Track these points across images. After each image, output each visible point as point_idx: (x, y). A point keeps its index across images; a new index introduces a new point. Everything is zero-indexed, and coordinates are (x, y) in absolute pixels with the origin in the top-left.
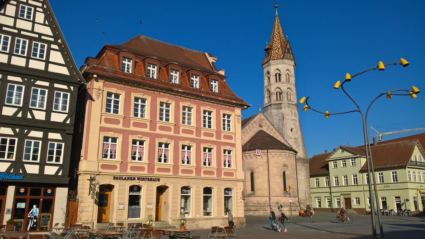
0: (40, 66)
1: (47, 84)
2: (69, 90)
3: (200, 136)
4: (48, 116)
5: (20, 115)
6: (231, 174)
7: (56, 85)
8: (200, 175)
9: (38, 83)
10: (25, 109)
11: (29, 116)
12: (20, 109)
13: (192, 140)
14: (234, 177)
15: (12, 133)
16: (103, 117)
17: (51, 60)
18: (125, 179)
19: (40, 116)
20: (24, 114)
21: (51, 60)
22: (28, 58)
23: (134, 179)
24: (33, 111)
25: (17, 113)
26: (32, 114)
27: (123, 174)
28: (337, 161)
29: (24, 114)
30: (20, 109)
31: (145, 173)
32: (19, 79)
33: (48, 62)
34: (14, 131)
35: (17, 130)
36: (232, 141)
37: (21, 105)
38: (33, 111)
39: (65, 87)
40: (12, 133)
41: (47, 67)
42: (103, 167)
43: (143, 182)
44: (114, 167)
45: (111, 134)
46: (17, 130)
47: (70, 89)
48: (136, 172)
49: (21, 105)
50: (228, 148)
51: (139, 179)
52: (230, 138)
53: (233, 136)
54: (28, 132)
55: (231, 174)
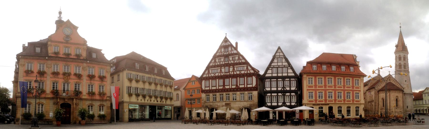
0: (286, 75)
1: (289, 79)
2: (295, 80)
3: (345, 88)
4: (290, 88)
5: (283, 89)
6: (359, 102)
7: (291, 79)
8: (354, 102)
9: (286, 79)
10: (284, 87)
11: (285, 89)
12: (282, 88)
13: (342, 90)
14: (360, 103)
15: (282, 95)
16: (308, 86)
17: (288, 72)
18: (317, 105)
19: (288, 89)
20: (284, 89)
21: (288, 72)
22: (282, 73)
23: (320, 105)
24: (286, 88)
25: (282, 89)
26: (286, 89)
27: (316, 103)
28: (426, 94)
29: (284, 89)
30: (282, 88)
31: (324, 102)
32: (281, 80)
33: (288, 73)
34: (282, 94)
35: (283, 94)
36: (359, 89)
37: (282, 87)
38: (286, 88)
39: (294, 79)
40: (282, 95)
41: (288, 74)
42: (309, 101)
43: (323, 106)
44: (313, 101)
45: (311, 91)
46: (283, 94)
47: (295, 79)
48: (320, 103)
49: (282, 87)
50: (357, 92)
51: (321, 105)
52: (359, 88)
53: (360, 87)
54: (286, 94)
55: (359, 102)
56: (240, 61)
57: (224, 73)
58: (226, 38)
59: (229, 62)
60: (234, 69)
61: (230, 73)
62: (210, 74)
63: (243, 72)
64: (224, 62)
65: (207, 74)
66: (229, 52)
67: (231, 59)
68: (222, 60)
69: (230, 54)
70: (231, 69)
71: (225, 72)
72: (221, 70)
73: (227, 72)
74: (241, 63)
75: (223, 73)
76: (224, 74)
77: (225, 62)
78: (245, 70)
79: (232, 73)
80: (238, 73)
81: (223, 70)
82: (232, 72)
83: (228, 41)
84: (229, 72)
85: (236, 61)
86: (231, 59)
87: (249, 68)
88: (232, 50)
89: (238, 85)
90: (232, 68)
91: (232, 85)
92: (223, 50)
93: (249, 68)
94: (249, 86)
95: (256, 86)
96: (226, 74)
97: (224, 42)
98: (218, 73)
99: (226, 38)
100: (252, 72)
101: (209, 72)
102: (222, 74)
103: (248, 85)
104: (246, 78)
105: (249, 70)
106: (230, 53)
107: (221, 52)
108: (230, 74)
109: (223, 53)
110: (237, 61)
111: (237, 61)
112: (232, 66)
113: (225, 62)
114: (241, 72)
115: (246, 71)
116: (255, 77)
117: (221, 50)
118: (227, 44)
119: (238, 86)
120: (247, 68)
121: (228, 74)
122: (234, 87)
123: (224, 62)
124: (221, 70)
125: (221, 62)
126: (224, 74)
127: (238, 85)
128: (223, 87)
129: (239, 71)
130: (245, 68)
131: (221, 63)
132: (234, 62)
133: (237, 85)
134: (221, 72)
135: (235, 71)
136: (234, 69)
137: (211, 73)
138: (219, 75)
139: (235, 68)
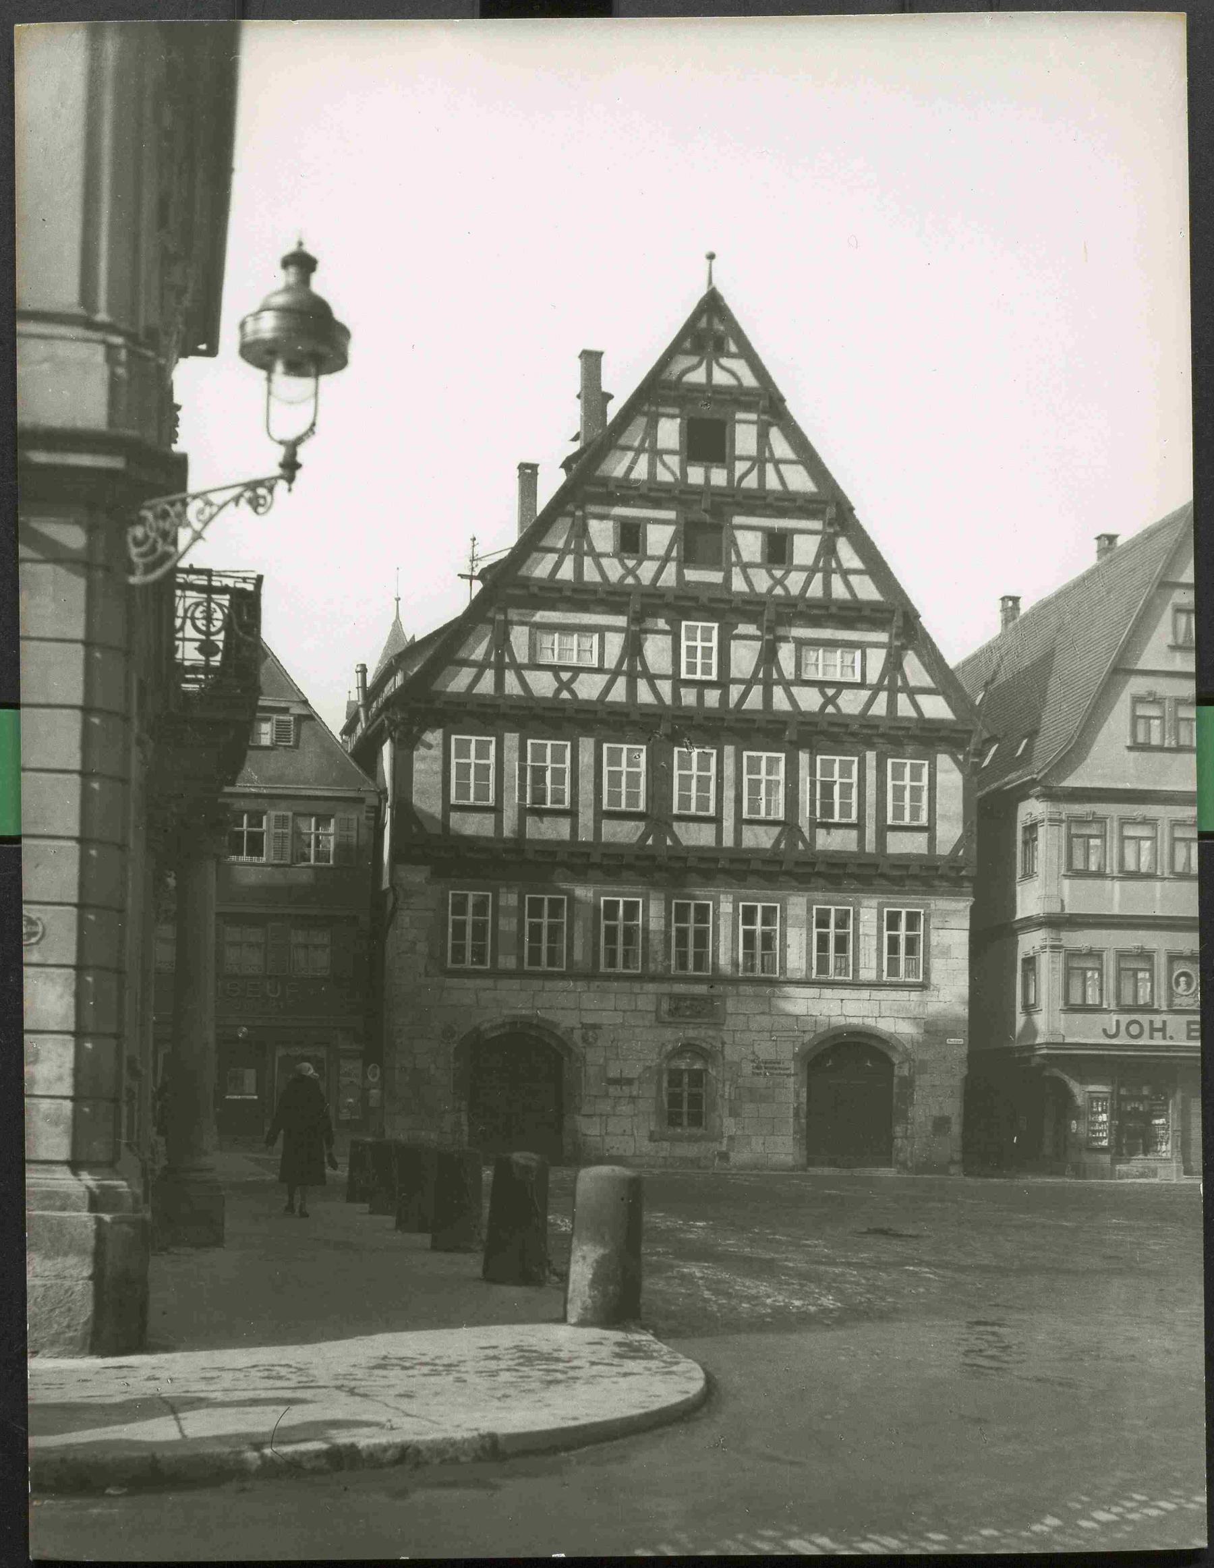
56: (839, 590)
57: (665, 687)
58: (712, 305)
59: (728, 579)
60: (768, 656)
61: (735, 691)
62: (519, 668)
63: (851, 703)
64: (671, 567)
65: (481, 667)
66: (740, 467)
67: (750, 545)
68: (659, 538)
69: (749, 494)
70: (744, 657)
71: (678, 683)
72: (633, 648)
73: (702, 685)
74: (843, 605)
75: (651, 679)
76: (668, 700)
77: (692, 575)
78: (876, 689)
79: (755, 701)
80: (809, 700)
81: (656, 651)
82: (749, 683)
83: (733, 348)
84: (723, 683)
85: (795, 582)
86: (750, 545)
87: (914, 670)
88: (761, 459)
89: (799, 830)
90: (757, 645)
91: (740, 821)
92: (669, 432)
93: (914, 670)
94: (901, 844)
95: (961, 853)
96: (689, 697)
97: (687, 344)
98: (602, 680)
99: (712, 305)
100: (936, 708)
101: (502, 642)
102: (645, 695)
103: (891, 837)
104: (871, 756)
105: (912, 692)
106: (751, 482)
107: (656, 454)
108: (731, 706)
109: (673, 461)
110: (803, 575)
111: (803, 575)
112: (751, 629)
113: (692, 575)
114: (840, 701)
115: (883, 696)
116: (956, 761)
117: (651, 430)
118: (721, 378)
119: (804, 841)
120: (894, 665)
121: (712, 698)
122: (761, 839)
123: (671, 567)
124: (633, 648)
125: (643, 557)
126: (668, 700)
127: (804, 821)
128: (642, 825)
129: (821, 685)
130: (877, 659)
131: (647, 571)
132: (780, 582)
133: (789, 826)
134: (632, 666)
135: (787, 685)
136: (768, 656)
137: (522, 657)
138: (610, 698)
139: (786, 653)
